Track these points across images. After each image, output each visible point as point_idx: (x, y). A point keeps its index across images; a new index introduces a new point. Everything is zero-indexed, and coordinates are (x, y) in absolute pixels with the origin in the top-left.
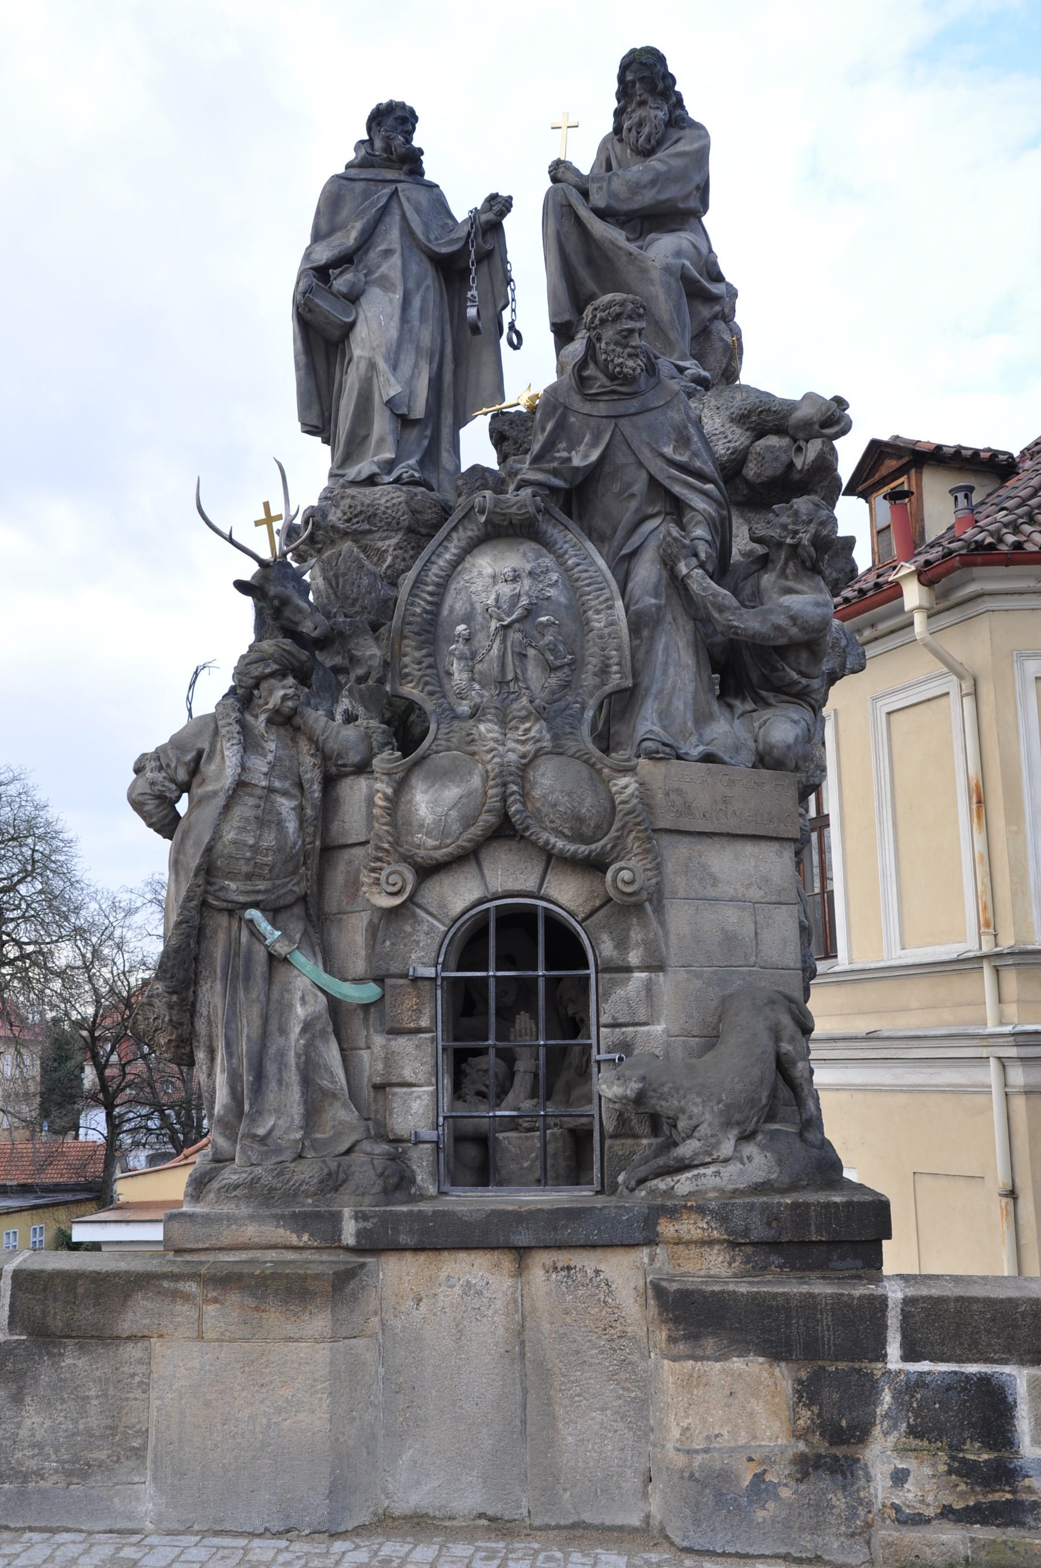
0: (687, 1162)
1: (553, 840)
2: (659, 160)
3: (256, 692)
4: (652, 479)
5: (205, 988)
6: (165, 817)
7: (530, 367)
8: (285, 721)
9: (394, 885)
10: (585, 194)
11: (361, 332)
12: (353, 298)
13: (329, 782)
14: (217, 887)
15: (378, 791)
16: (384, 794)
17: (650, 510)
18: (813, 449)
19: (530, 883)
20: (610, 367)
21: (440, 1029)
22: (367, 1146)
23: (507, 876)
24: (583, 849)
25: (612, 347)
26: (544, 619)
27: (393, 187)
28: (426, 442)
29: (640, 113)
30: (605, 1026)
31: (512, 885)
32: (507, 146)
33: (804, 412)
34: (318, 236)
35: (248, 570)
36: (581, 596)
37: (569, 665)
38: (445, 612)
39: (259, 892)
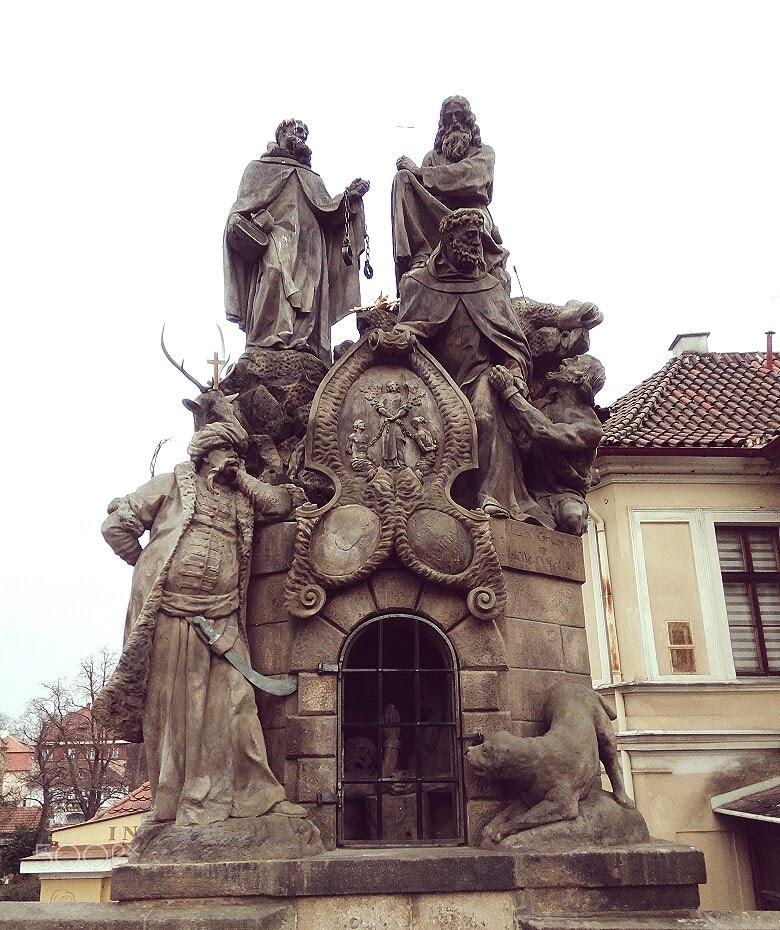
0: (543, 820)
1: (429, 570)
2: (466, 162)
3: (205, 459)
4: (483, 337)
5: (157, 682)
6: (131, 547)
7: (379, 286)
8: (227, 480)
9: (311, 600)
10: (420, 179)
11: (272, 252)
12: (267, 231)
13: (258, 527)
14: (172, 598)
15: (300, 530)
16: (304, 532)
17: (480, 358)
18: (573, 337)
19: (409, 603)
20: (459, 257)
21: (340, 712)
22: (287, 807)
23: (391, 596)
24: (451, 578)
25: (461, 244)
26: (418, 419)
27: (292, 169)
28: (311, 330)
29: (456, 134)
30: (466, 711)
31: (394, 604)
32: (367, 151)
33: (568, 312)
34: (243, 195)
35: (194, 394)
36: (442, 405)
37: (433, 451)
38: (346, 412)
39: (205, 603)
